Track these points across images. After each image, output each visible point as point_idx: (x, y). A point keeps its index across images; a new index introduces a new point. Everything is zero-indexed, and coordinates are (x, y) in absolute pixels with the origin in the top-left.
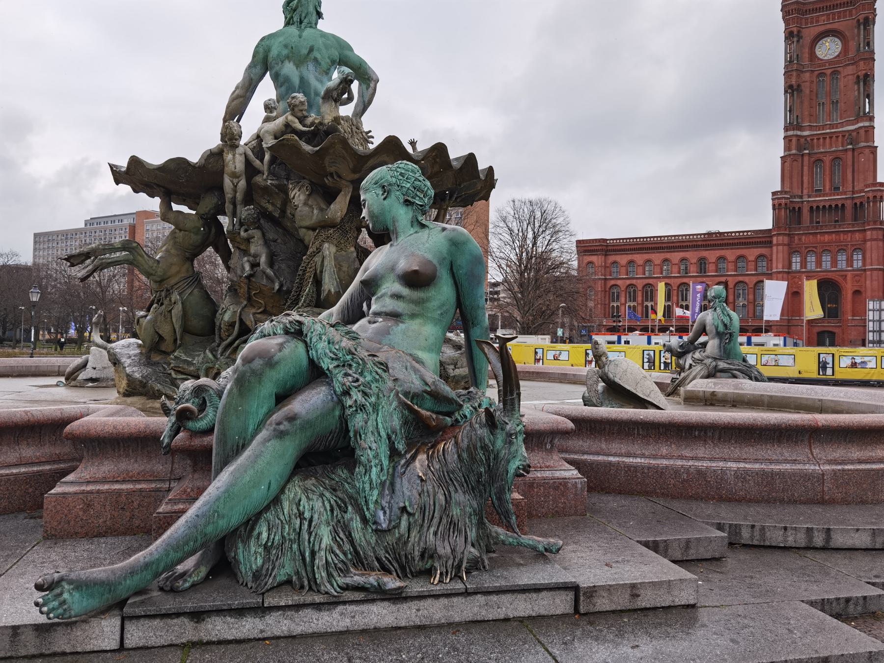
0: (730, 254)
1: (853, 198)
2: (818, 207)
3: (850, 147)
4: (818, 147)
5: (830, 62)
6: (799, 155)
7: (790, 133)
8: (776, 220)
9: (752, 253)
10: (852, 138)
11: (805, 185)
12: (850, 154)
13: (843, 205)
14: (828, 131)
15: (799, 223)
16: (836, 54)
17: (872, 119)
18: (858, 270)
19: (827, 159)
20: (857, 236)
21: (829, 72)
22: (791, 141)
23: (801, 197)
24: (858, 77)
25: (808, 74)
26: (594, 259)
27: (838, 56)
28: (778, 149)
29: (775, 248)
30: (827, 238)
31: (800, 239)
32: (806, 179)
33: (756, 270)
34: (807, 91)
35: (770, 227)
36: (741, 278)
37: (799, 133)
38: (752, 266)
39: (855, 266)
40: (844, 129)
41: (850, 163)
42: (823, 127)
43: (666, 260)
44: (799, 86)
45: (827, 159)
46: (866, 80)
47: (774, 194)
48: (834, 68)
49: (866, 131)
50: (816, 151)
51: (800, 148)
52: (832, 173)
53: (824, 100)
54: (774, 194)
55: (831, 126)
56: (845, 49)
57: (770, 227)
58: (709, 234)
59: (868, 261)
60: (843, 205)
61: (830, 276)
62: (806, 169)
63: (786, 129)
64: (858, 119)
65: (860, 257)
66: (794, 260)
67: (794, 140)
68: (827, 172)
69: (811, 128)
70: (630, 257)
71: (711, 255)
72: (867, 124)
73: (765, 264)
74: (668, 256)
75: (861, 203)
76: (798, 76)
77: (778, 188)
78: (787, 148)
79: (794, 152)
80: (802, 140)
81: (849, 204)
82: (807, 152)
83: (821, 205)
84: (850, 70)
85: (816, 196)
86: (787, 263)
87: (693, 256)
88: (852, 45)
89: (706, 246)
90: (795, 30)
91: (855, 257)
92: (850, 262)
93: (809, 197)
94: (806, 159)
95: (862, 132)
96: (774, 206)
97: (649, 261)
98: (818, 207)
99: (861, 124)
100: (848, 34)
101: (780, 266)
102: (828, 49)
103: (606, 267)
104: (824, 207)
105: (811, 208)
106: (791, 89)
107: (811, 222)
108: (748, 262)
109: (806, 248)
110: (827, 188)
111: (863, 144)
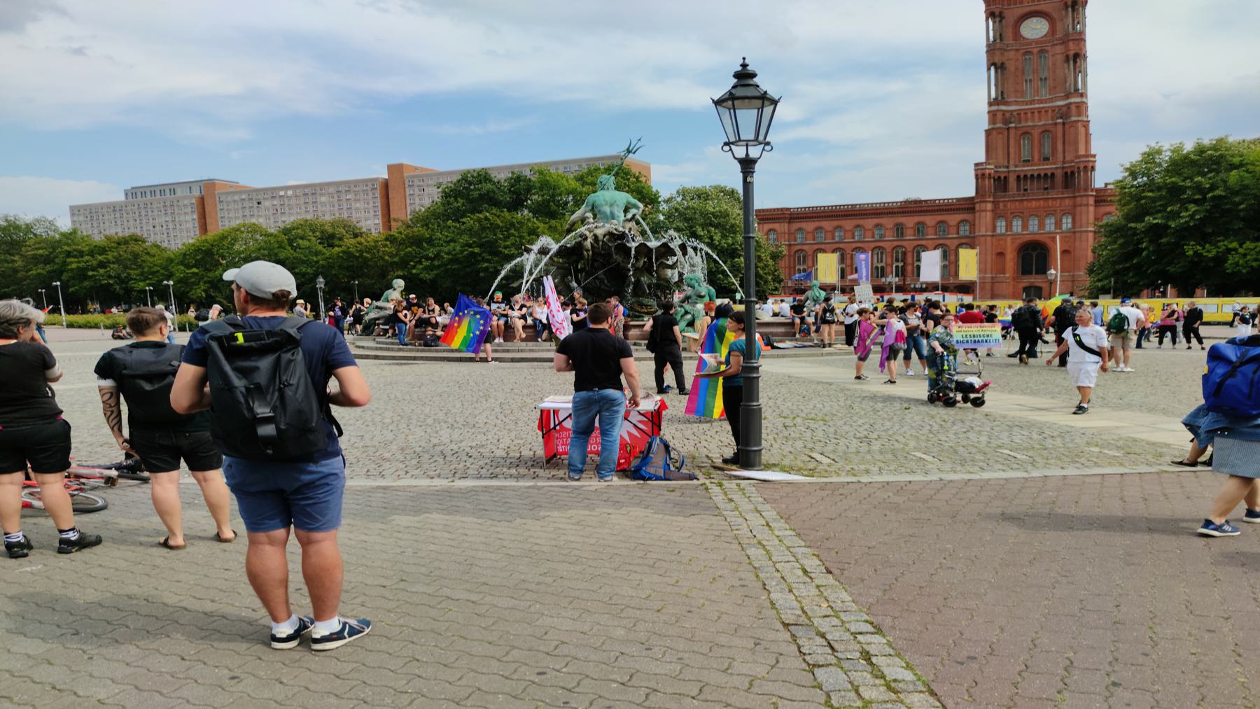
0: (930, 220)
4: (1026, 121)
5: (1037, 41)
6: (1003, 126)
9: (953, 219)
10: (1065, 113)
11: (1012, 156)
12: (1060, 128)
13: (1053, 174)
15: (1005, 189)
18: (1068, 231)
19: (1036, 132)
20: (1067, 202)
21: (1035, 51)
24: (1067, 56)
25: (1012, 54)
26: (776, 226)
30: (1034, 204)
32: (1012, 150)
34: (1013, 69)
35: (970, 192)
37: (1003, 108)
38: (953, 230)
39: (1064, 227)
41: (1060, 135)
42: (1032, 102)
43: (858, 226)
45: (1036, 132)
46: (1077, 58)
48: (1041, 47)
50: (1023, 124)
52: (1041, 145)
55: (1041, 102)
56: (1053, 30)
57: (970, 192)
58: (907, 202)
59: (1078, 224)
60: (1053, 174)
61: (1037, 237)
63: (990, 104)
64: (1067, 96)
65: (1070, 220)
66: (998, 224)
67: (999, 116)
68: (1036, 142)
69: (1017, 103)
70: (817, 224)
71: (910, 221)
72: (1078, 100)
74: (861, 222)
75: (1073, 173)
76: (1002, 54)
77: (982, 158)
79: (998, 125)
80: (1007, 115)
81: (1059, 173)
84: (1059, 49)
86: (990, 227)
87: (889, 222)
88: (1059, 26)
91: (1064, 221)
92: (1058, 224)
94: (1012, 132)
95: (1073, 108)
96: (977, 176)
97: (839, 227)
99: (1072, 100)
100: (1054, 15)
101: (983, 229)
102: (1035, 29)
103: (789, 234)
104: (1032, 176)
105: (1018, 177)
107: (1018, 189)
108: (949, 226)
110: (1036, 158)
111: (1074, 119)
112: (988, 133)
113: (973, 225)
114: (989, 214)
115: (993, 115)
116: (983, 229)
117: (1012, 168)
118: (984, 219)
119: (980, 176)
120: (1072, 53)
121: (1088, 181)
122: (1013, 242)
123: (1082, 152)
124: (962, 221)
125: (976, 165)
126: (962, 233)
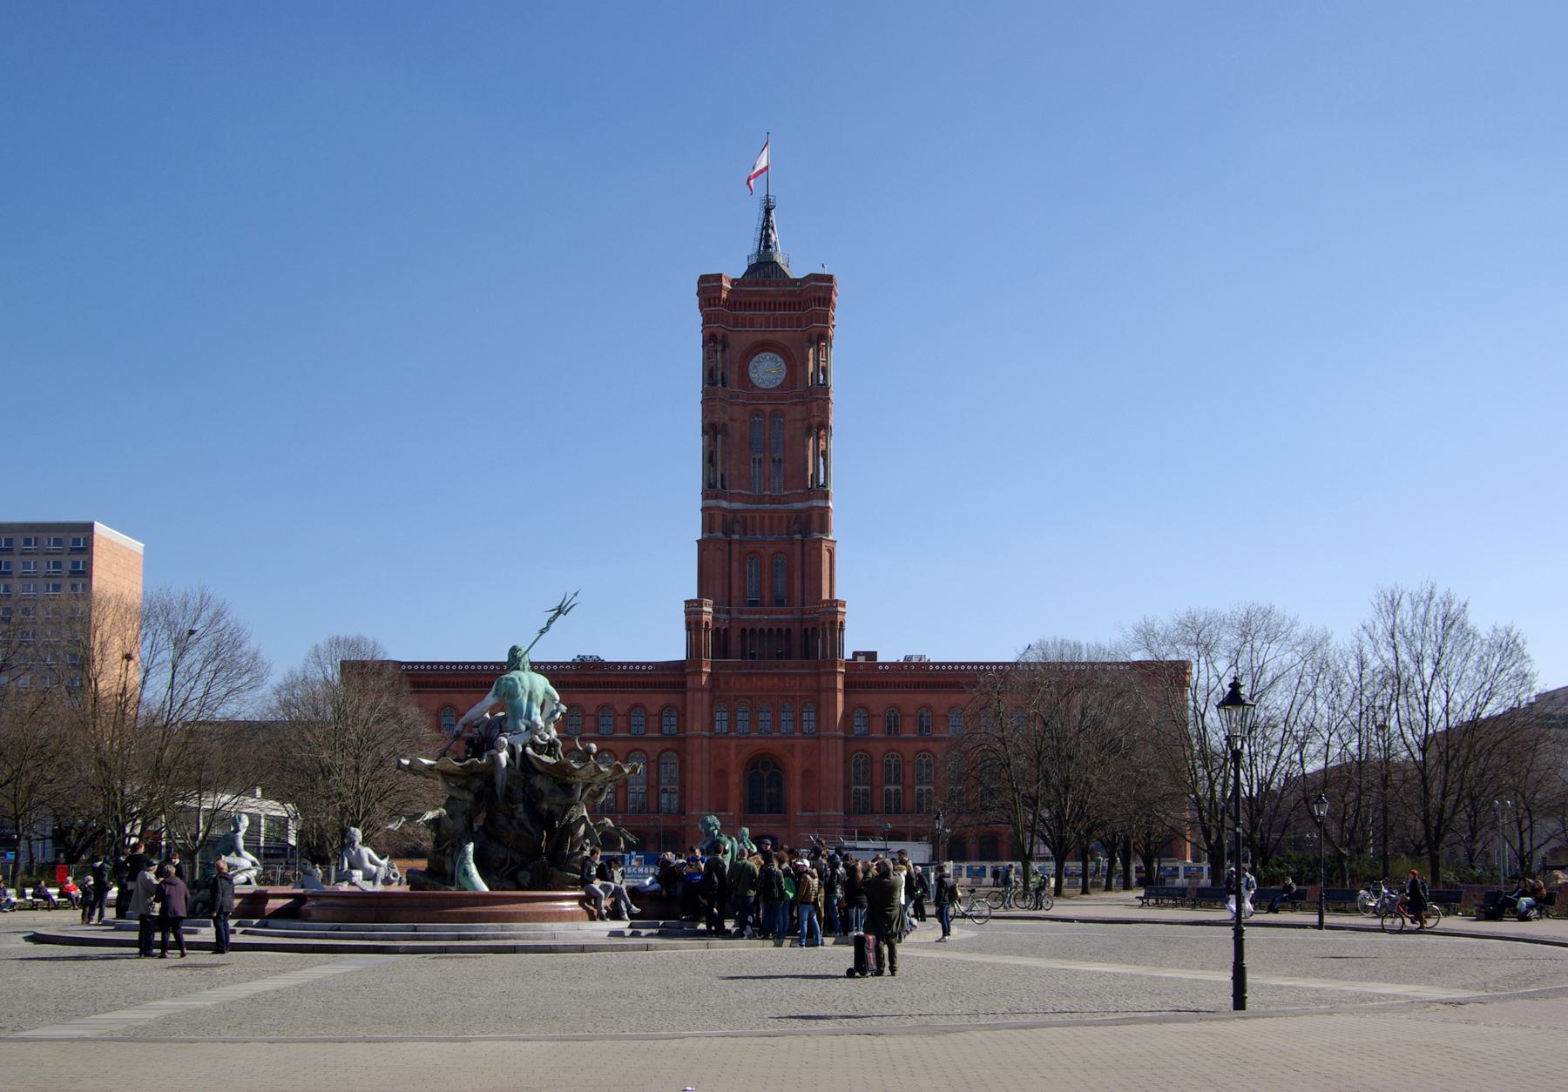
0: (621, 701)
1: (802, 621)
2: (753, 630)
3: (798, 537)
5: (770, 394)
7: (712, 503)
8: (693, 647)
9: (654, 701)
12: (798, 547)
13: (789, 630)
17: (826, 496)
27: (782, 386)
28: (694, 529)
29: (689, 694)
33: (660, 730)
36: (637, 744)
37: (724, 504)
40: (789, 506)
44: (724, 425)
51: (727, 531)
53: (761, 455)
55: (773, 500)
60: (789, 630)
62: (735, 565)
72: (821, 504)
73: (674, 720)
78: (708, 525)
82: (736, 537)
83: (758, 627)
85: (751, 613)
90: (719, 332)
93: (741, 612)
94: (735, 548)
98: (753, 630)
101: (697, 725)
102: (767, 371)
105: (743, 630)
106: (711, 430)
109: (737, 698)
111: (816, 535)
113: (682, 716)
114: (706, 695)
115: (708, 514)
116: (697, 725)
117: (735, 615)
118: (698, 706)
119: (693, 623)
120: (817, 420)
121: (836, 646)
123: (826, 596)
124: (667, 706)
125: (687, 602)
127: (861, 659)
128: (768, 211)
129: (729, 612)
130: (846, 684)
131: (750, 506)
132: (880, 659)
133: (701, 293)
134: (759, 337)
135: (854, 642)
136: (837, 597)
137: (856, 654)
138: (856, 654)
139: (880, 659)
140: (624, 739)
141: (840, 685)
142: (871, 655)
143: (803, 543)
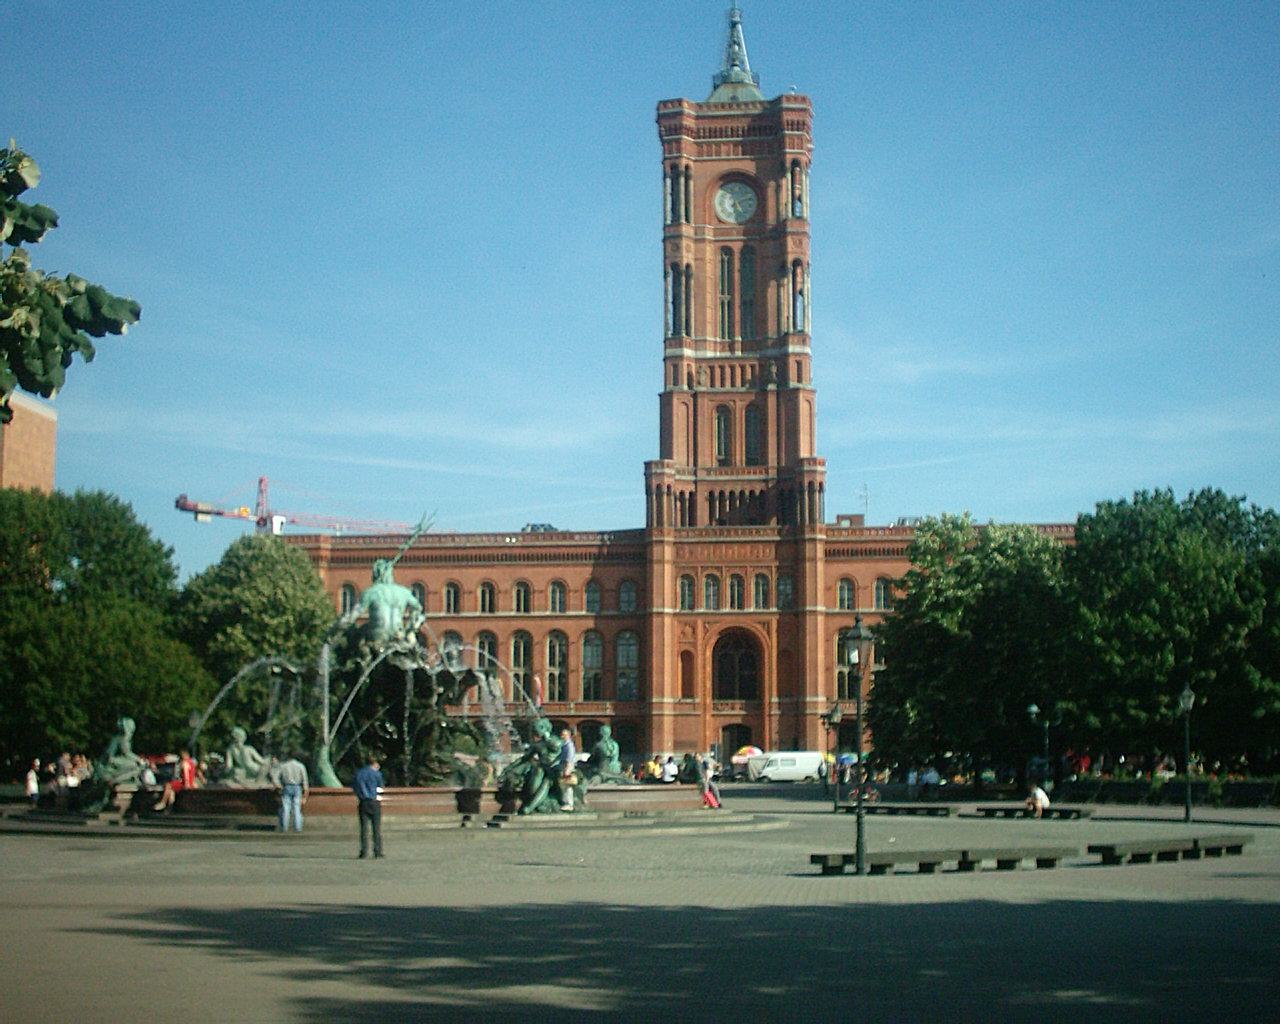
2: (722, 493)
12: (772, 401)
14: (739, 353)
15: (693, 522)
16: (748, 216)
22: (676, 367)
23: (695, 474)
31: (691, 553)
37: (688, 352)
44: (688, 266)
47: (648, 465)
49: (799, 363)
54: (648, 465)
71: (540, 577)
87: (504, 578)
89: (528, 558)
105: (711, 494)
111: (793, 384)
112: (666, 399)
117: (702, 475)
122: (706, 631)
123: (804, 454)
124: (624, 581)
126: (624, 607)
127: (845, 524)
128: (734, 25)
129: (695, 474)
130: (827, 553)
131: (718, 354)
132: (868, 523)
133: (660, 118)
134: (726, 167)
135: (834, 505)
136: (815, 455)
137: (840, 518)
138: (840, 518)
139: (868, 523)
140: (612, 617)
141: (820, 554)
142: (856, 519)
143: (778, 394)
